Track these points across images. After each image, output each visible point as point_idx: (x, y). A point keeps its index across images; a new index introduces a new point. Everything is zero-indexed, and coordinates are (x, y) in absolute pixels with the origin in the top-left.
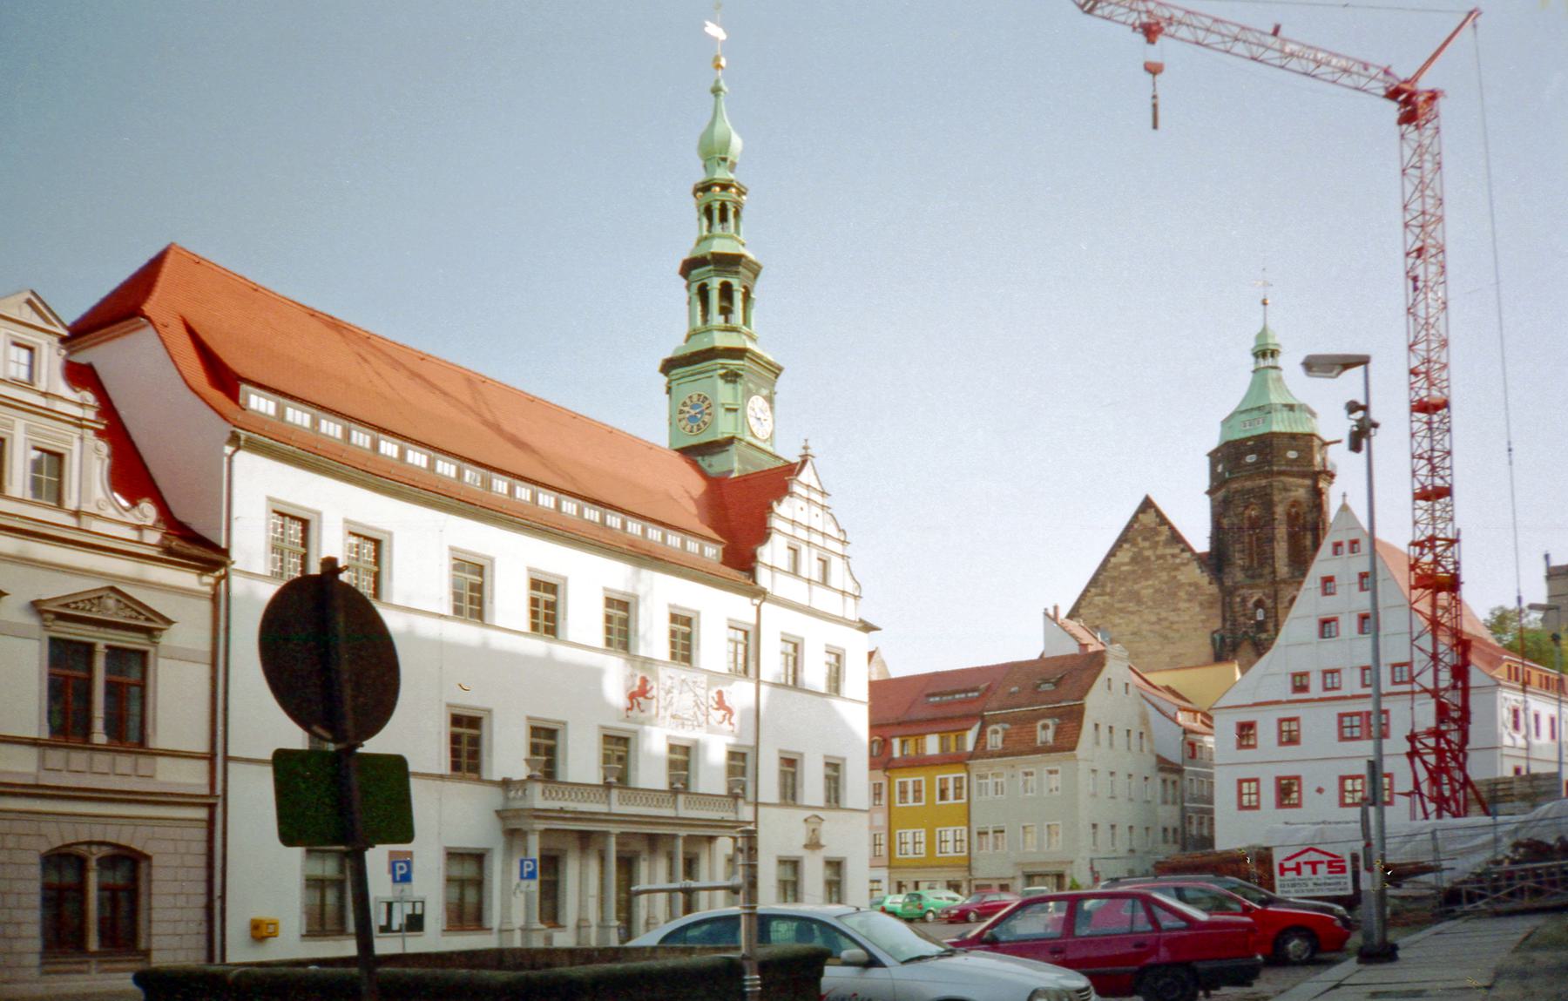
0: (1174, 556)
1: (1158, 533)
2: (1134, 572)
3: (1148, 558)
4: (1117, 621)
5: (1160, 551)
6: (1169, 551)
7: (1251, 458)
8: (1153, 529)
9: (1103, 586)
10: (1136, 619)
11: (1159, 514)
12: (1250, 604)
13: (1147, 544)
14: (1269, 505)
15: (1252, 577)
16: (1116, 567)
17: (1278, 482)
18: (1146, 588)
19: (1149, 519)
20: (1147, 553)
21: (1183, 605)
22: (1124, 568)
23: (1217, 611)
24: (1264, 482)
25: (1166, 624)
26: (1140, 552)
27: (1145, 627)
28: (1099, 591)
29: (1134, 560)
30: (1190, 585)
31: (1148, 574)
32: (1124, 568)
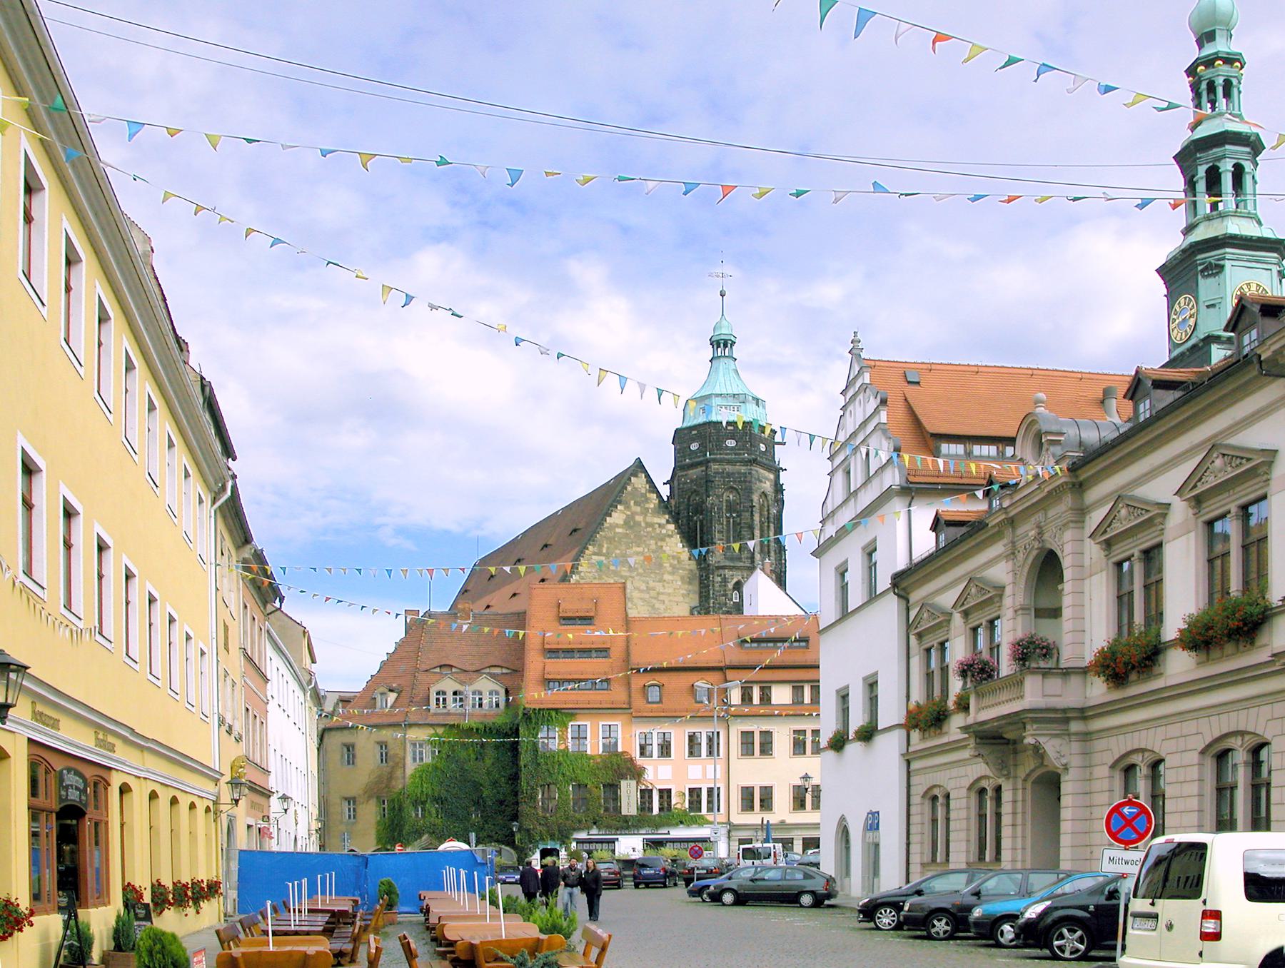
0: (660, 525)
1: (647, 500)
2: (626, 535)
3: (639, 524)
5: (649, 519)
6: (656, 520)
7: (731, 443)
8: (644, 495)
9: (601, 546)
11: (649, 480)
12: (730, 586)
13: (638, 509)
14: (750, 491)
15: (732, 559)
17: (755, 468)
19: (639, 482)
20: (639, 518)
21: (667, 577)
22: (618, 530)
23: (696, 587)
24: (743, 469)
25: (653, 593)
26: (634, 514)
28: (596, 550)
30: (673, 557)
31: (639, 540)
32: (618, 530)
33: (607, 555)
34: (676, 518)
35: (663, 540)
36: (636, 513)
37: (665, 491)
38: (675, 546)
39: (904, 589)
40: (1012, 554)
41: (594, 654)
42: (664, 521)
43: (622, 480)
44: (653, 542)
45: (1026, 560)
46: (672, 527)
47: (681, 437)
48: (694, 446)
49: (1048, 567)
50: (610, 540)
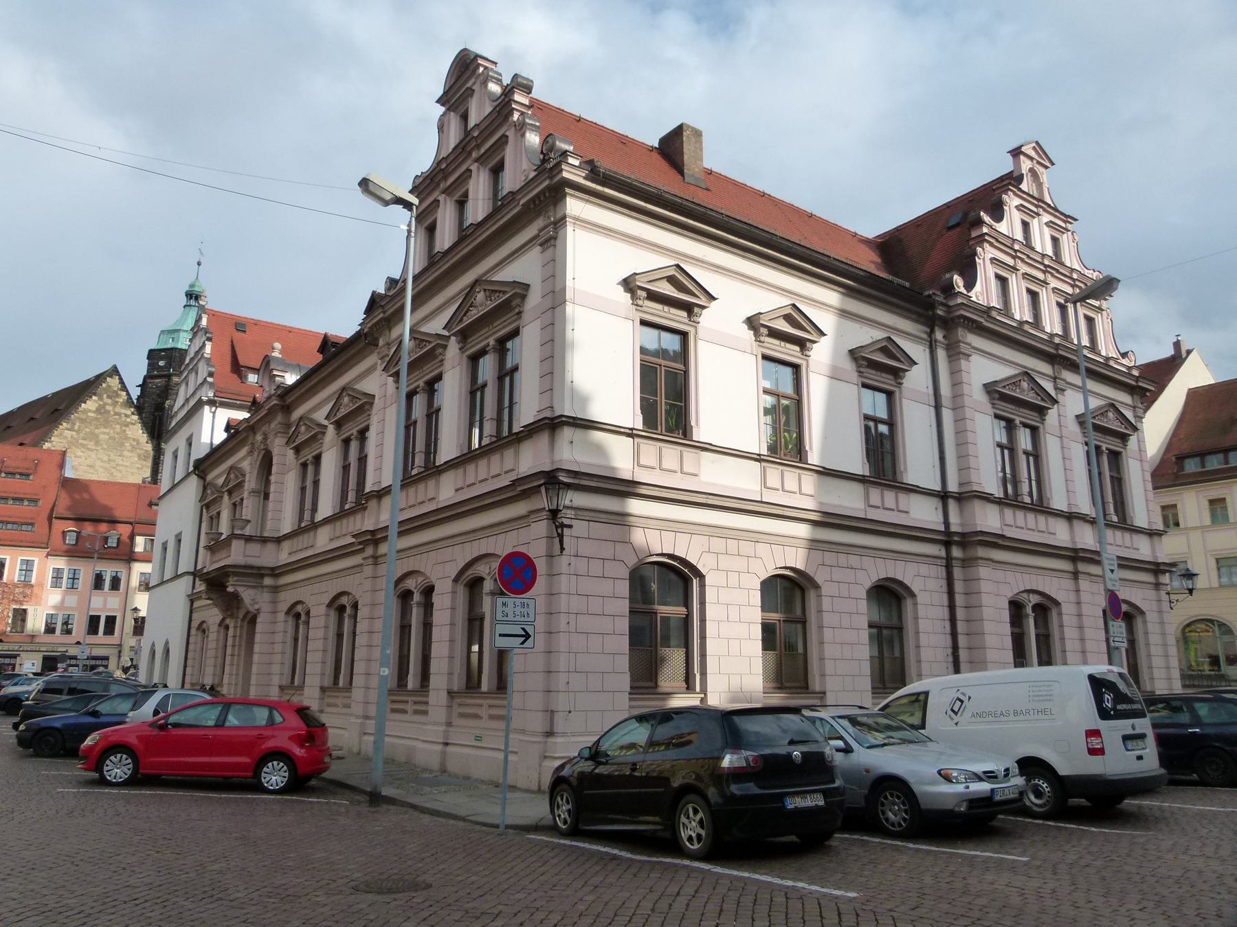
0: (126, 416)
1: (118, 396)
4: (79, 453)
5: (118, 409)
6: (123, 411)
10: (93, 455)
11: (122, 382)
13: (109, 401)
16: (86, 411)
18: (103, 433)
19: (113, 382)
20: (108, 408)
21: (126, 453)
23: (149, 463)
25: (113, 464)
27: (98, 463)
29: (98, 411)
31: (106, 424)
33: (78, 432)
34: (139, 409)
35: (127, 426)
36: (106, 404)
37: (135, 393)
38: (138, 433)
39: (203, 471)
40: (251, 452)
41: (26, 503)
42: (129, 412)
43: (100, 378)
44: (118, 427)
45: (258, 456)
46: (136, 417)
47: (153, 355)
48: (161, 363)
49: (266, 463)
50: (82, 421)
